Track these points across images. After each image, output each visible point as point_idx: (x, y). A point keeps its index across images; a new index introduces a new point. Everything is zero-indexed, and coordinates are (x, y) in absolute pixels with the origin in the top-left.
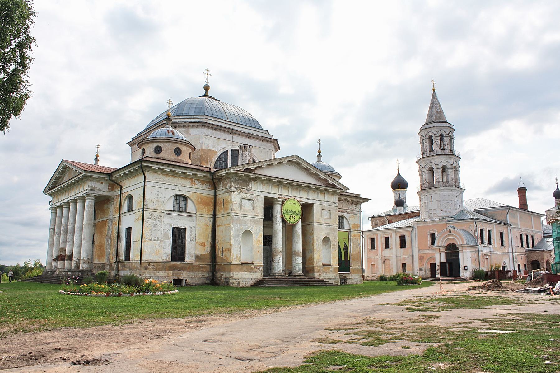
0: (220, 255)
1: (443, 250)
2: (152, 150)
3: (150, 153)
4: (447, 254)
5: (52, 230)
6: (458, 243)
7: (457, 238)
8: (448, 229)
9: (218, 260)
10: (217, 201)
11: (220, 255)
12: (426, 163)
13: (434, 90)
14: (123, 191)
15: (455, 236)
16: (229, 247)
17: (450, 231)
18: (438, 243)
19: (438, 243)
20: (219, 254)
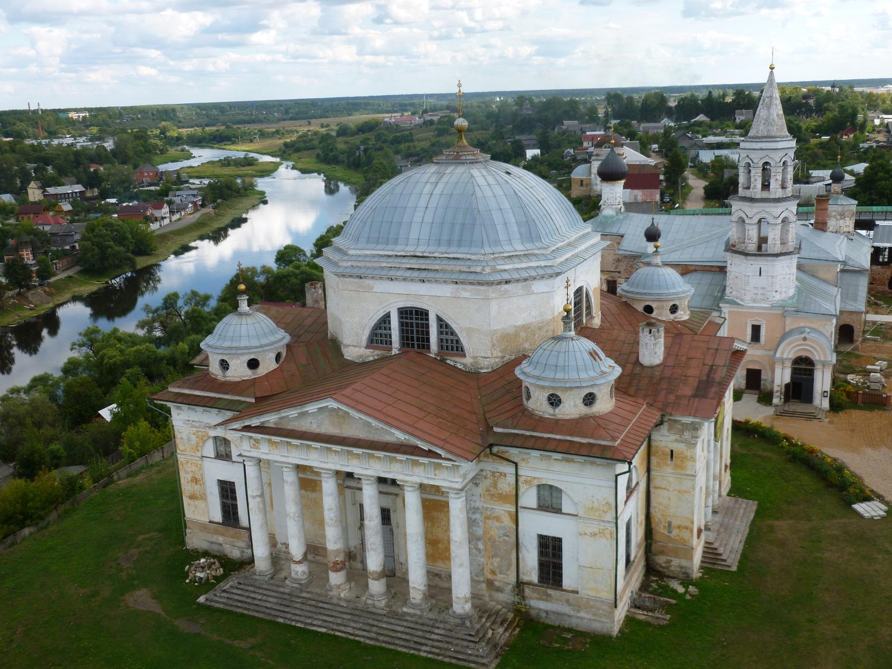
0: (666, 532)
1: (789, 364)
2: (580, 402)
3: (575, 406)
4: (795, 371)
5: (258, 499)
6: (816, 357)
7: (816, 350)
8: (803, 336)
9: (656, 537)
10: (653, 449)
11: (666, 532)
12: (755, 210)
13: (772, 68)
14: (520, 472)
15: (816, 350)
16: (688, 524)
17: (805, 339)
18: (783, 353)
19: (783, 353)
20: (660, 529)
